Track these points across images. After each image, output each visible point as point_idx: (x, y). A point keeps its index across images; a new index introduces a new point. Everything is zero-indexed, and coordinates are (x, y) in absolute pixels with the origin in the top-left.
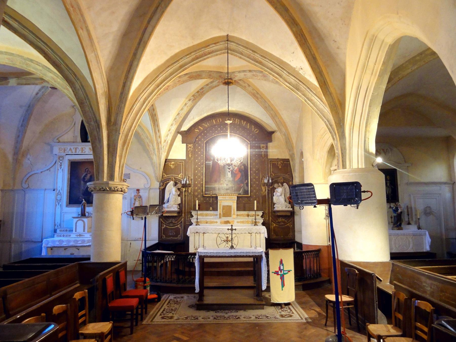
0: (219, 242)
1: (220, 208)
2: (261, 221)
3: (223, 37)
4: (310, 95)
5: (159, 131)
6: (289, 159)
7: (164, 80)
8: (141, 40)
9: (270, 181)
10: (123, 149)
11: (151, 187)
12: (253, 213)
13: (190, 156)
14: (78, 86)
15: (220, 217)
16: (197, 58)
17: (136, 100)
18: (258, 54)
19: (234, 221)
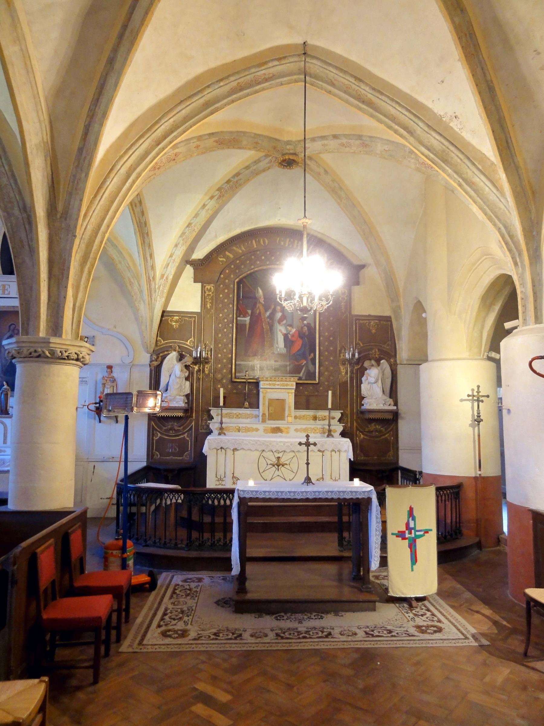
0: (263, 466)
1: (264, 404)
2: (340, 428)
3: (296, 46)
4: (471, 172)
5: (151, 256)
6: (390, 317)
7: (171, 131)
8: (125, 27)
9: (357, 355)
10: (82, 271)
11: (136, 363)
12: (325, 413)
13: (208, 306)
15: (264, 421)
16: (241, 88)
17: (112, 170)
18: (367, 84)
19: (289, 428)
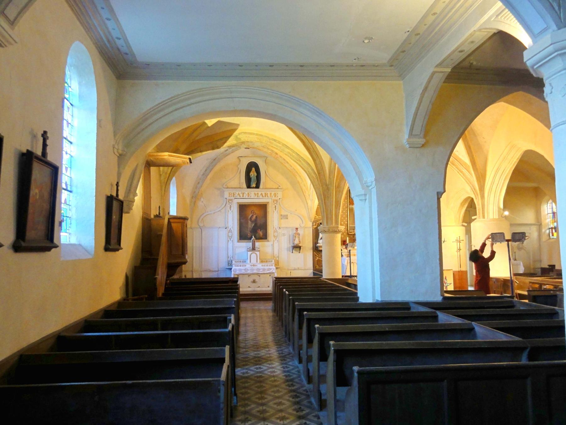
14: (318, 162)
